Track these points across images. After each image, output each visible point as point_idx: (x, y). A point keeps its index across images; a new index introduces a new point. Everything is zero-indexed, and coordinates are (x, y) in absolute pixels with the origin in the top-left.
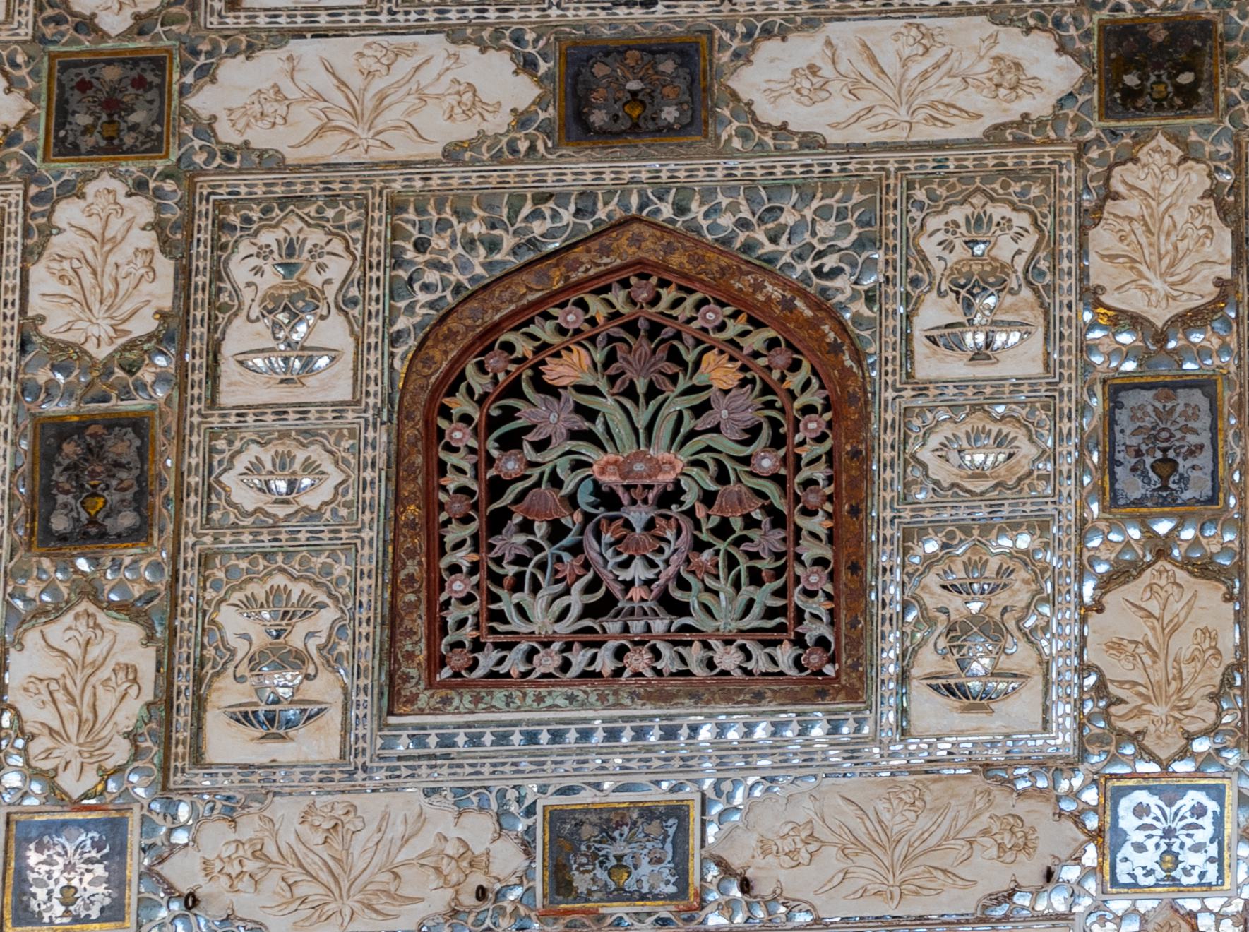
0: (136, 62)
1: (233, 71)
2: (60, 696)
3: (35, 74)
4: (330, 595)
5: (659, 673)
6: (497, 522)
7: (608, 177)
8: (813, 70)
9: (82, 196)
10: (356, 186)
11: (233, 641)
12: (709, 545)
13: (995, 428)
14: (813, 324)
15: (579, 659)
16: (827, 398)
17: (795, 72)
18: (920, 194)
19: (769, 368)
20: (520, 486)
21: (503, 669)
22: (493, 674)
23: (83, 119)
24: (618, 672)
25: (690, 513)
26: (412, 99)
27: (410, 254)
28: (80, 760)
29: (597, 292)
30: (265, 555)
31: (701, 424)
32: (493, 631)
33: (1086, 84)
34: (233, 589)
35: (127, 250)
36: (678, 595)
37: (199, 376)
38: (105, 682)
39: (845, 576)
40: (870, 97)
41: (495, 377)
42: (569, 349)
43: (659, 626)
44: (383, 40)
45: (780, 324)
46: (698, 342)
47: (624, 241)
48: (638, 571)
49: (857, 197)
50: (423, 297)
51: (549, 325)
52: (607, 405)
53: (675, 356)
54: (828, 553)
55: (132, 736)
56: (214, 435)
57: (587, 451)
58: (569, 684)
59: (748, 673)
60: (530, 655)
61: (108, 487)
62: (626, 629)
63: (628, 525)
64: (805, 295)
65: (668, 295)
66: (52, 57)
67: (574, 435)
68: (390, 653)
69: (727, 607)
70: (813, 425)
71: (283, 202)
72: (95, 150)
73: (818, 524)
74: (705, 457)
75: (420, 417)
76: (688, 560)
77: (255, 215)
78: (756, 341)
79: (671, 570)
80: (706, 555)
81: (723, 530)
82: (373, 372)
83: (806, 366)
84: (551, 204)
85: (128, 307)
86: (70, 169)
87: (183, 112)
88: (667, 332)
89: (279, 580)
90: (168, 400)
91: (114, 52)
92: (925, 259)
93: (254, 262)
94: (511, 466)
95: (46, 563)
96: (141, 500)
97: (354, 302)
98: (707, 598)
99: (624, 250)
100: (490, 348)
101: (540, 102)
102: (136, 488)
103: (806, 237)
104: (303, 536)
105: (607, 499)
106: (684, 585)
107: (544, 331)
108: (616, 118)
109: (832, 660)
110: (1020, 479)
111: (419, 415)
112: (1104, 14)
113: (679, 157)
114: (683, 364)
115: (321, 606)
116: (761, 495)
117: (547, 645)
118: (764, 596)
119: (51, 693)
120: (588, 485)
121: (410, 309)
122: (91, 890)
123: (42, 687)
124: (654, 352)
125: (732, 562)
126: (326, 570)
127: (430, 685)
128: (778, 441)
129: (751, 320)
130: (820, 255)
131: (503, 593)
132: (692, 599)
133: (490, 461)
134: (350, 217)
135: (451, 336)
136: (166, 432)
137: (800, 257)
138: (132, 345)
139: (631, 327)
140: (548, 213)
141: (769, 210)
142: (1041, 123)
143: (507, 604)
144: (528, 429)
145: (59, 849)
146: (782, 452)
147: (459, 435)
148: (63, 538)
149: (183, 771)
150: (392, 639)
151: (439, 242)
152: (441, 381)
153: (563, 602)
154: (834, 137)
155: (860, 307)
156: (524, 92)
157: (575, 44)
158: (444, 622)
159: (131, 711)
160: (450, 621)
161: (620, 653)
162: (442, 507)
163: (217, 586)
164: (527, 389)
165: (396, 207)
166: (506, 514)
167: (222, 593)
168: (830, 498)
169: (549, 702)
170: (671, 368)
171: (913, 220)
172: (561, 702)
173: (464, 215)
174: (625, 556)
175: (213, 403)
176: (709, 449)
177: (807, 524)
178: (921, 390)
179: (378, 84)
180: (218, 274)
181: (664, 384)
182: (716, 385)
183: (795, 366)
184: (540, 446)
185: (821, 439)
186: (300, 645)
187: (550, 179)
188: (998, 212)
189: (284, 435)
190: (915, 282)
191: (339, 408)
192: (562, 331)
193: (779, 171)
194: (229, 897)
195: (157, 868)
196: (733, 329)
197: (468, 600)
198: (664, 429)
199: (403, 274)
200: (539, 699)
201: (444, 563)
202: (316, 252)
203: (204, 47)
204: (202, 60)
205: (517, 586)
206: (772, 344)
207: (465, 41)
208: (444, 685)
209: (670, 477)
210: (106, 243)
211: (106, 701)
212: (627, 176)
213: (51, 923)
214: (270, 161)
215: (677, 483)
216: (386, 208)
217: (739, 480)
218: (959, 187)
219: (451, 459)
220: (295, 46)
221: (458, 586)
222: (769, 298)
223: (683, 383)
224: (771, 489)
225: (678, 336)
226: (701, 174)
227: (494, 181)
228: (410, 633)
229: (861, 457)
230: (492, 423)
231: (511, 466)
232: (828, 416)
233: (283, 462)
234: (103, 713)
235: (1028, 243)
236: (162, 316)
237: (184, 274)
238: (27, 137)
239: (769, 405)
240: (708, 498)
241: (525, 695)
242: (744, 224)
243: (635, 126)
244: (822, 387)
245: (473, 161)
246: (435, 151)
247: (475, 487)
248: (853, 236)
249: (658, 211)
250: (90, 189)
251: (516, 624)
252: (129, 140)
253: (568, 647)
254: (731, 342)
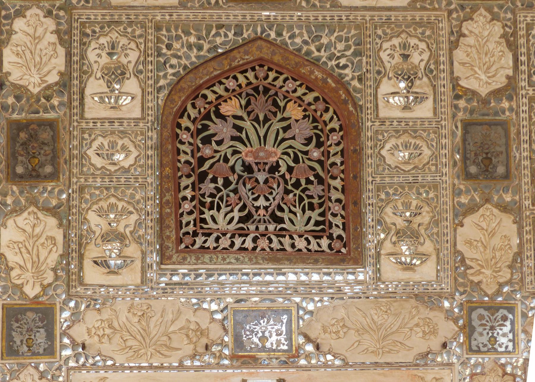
12: (292, 191)
14: (336, 90)
16: (341, 126)
19: (315, 111)
25: (283, 176)
29: (242, 72)
31: (288, 135)
39: (351, 207)
41: (200, 110)
42: (230, 98)
46: (285, 97)
47: (254, 49)
49: (353, 32)
51: (222, 87)
53: (275, 104)
54: (342, 197)
64: (331, 76)
67: (233, 138)
73: (337, 183)
74: (290, 151)
78: (310, 98)
81: (297, 185)
84: (224, 30)
88: (272, 92)
92: (382, 62)
100: (197, 97)
103: (332, 51)
110: (424, 165)
116: (312, 169)
124: (267, 101)
128: (319, 145)
129: (307, 88)
130: (338, 58)
139: (256, 89)
140: (222, 34)
141: (316, 36)
146: (322, 149)
168: (343, 172)
171: (377, 44)
176: (290, 147)
177: (333, 183)
178: (383, 123)
182: (294, 117)
183: (327, 110)
185: (338, 144)
192: (227, 90)
193: (320, 18)
196: (301, 91)
206: (316, 99)
209: (275, 159)
212: (256, 18)
215: (277, 162)
217: (304, 162)
218: (396, 29)
222: (316, 77)
223: (279, 116)
225: (276, 94)
226: (287, 18)
229: (358, 152)
232: (341, 133)
239: (316, 128)
240: (290, 169)
242: (305, 42)
244: (339, 120)
248: (352, 50)
249: (269, 35)
254: (299, 98)
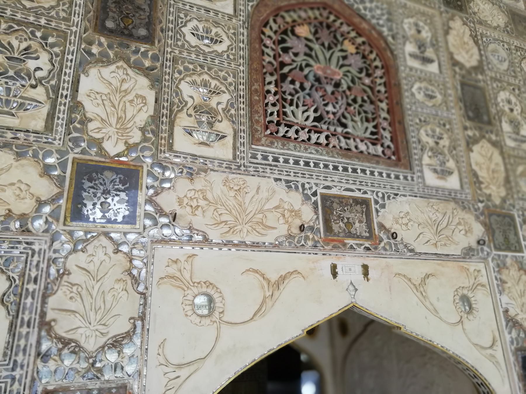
4: (227, 89)
6: (283, 77)
11: (186, 98)
20: (290, 67)
24: (327, 145)
28: (116, 136)
32: (284, 120)
34: (187, 76)
36: (344, 120)
52: (316, 47)
61: (134, 16)
65: (332, 18)
76: (346, 109)
78: (360, 40)
89: (206, 77)
102: (147, 20)
106: (345, 117)
116: (365, 91)
119: (103, 100)
122: (118, 206)
123: (98, 96)
131: (287, 105)
145: (101, 181)
149: (164, 152)
153: (306, 114)
164: (289, 33)
167: (182, 76)
169: (309, 151)
172: (314, 152)
174: (326, 102)
181: (333, 46)
186: (214, 106)
195: (154, 198)
197: (274, 105)
200: (306, 149)
205: (291, 104)
213: (94, 221)
215: (340, 80)
221: (271, 99)
223: (339, 47)
234: (129, 115)
240: (349, 88)
241: (301, 147)
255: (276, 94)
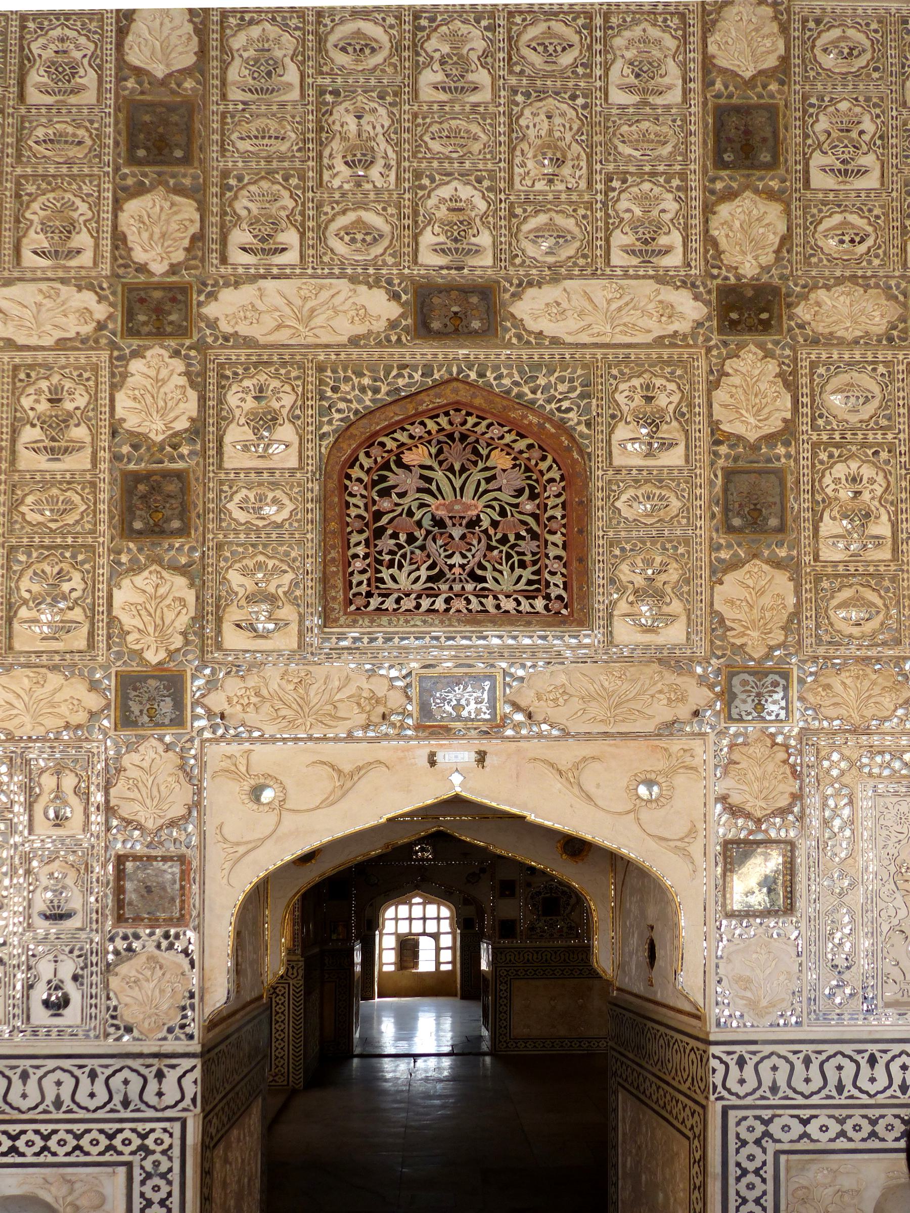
0: (171, 289)
1: (227, 295)
2: (143, 612)
3: (114, 293)
5: (470, 611)
6: (379, 533)
7: (440, 357)
8: (558, 304)
9: (144, 357)
10: (298, 357)
13: (658, 492)
15: (425, 603)
17: (547, 305)
18: (615, 372)
19: (529, 459)
20: (391, 515)
21: (384, 607)
22: (378, 609)
23: (142, 318)
24: (447, 610)
25: (485, 531)
26: (330, 312)
27: (329, 394)
30: (253, 545)
33: (709, 318)
35: (170, 386)
36: (479, 572)
37: (212, 452)
38: (168, 606)
40: (589, 320)
43: (469, 587)
44: (313, 281)
45: (535, 435)
46: (489, 445)
48: (457, 559)
49: (579, 372)
50: (337, 416)
52: (439, 475)
53: (475, 452)
54: (563, 553)
55: (184, 634)
56: (221, 483)
57: (428, 499)
58: (422, 614)
59: (519, 612)
60: (398, 601)
62: (451, 588)
63: (451, 536)
64: (550, 421)
65: (471, 420)
66: (124, 285)
68: (324, 597)
69: (507, 580)
70: (554, 488)
71: (256, 365)
72: (149, 334)
73: (558, 538)
74: (494, 503)
75: (336, 475)
77: (240, 371)
78: (522, 444)
79: (476, 559)
80: (496, 552)
81: (504, 540)
82: (310, 453)
83: (550, 458)
85: (172, 415)
86: (135, 343)
87: (199, 315)
88: (471, 439)
90: (197, 464)
91: (159, 283)
93: (240, 395)
94: (386, 504)
95: (131, 545)
96: (183, 513)
97: (298, 417)
98: (497, 575)
99: (449, 395)
101: (402, 315)
103: (552, 394)
104: (274, 536)
105: (439, 523)
107: (402, 437)
108: (446, 326)
109: (566, 607)
111: (335, 477)
112: (719, 281)
113: (482, 347)
114: (481, 456)
115: (285, 572)
117: (407, 595)
118: (527, 574)
120: (429, 516)
121: (330, 422)
125: (509, 556)
126: (287, 554)
127: (345, 613)
130: (560, 401)
131: (383, 569)
132: (488, 575)
133: (374, 502)
134: (294, 374)
135: (352, 437)
136: (197, 480)
137: (549, 401)
138: (176, 434)
142: (685, 336)
143: (385, 574)
144: (394, 487)
147: (356, 488)
148: (140, 532)
150: (325, 589)
151: (345, 388)
152: (346, 461)
154: (569, 339)
155: (582, 428)
156: (394, 310)
157: (421, 286)
158: (351, 582)
159: (183, 620)
160: (354, 582)
161: (448, 601)
162: (348, 524)
163: (226, 560)
165: (321, 369)
166: (383, 529)
168: (564, 526)
170: (474, 458)
173: (360, 375)
175: (220, 467)
176: (495, 499)
177: (551, 538)
179: (310, 304)
180: (221, 401)
182: (500, 467)
183: (544, 458)
184: (401, 495)
185: (558, 496)
187: (408, 357)
188: (658, 382)
189: (260, 484)
190: (613, 416)
191: (292, 471)
193: (536, 357)
194: (242, 715)
196: (508, 438)
197: (363, 571)
198: (470, 488)
199: (325, 404)
201: (350, 553)
202: (275, 391)
203: (210, 282)
204: (209, 288)
205: (391, 565)
206: (530, 447)
207: (360, 283)
208: (351, 613)
209: (475, 513)
210: (159, 382)
211: (169, 616)
214: (249, 342)
216: (315, 369)
219: (352, 500)
220: (262, 283)
221: (358, 565)
223: (481, 465)
224: (531, 521)
225: (477, 441)
227: (376, 357)
228: (334, 587)
230: (375, 483)
231: (386, 504)
233: (261, 498)
235: (676, 398)
236: (192, 420)
237: (202, 400)
238: (110, 326)
239: (529, 478)
240: (495, 524)
242: (516, 384)
243: (457, 330)
245: (365, 346)
246: (344, 339)
247: (365, 515)
250: (148, 354)
251: (390, 584)
252: (169, 329)
253: (419, 597)
254: (507, 445)
255: (366, 556)
